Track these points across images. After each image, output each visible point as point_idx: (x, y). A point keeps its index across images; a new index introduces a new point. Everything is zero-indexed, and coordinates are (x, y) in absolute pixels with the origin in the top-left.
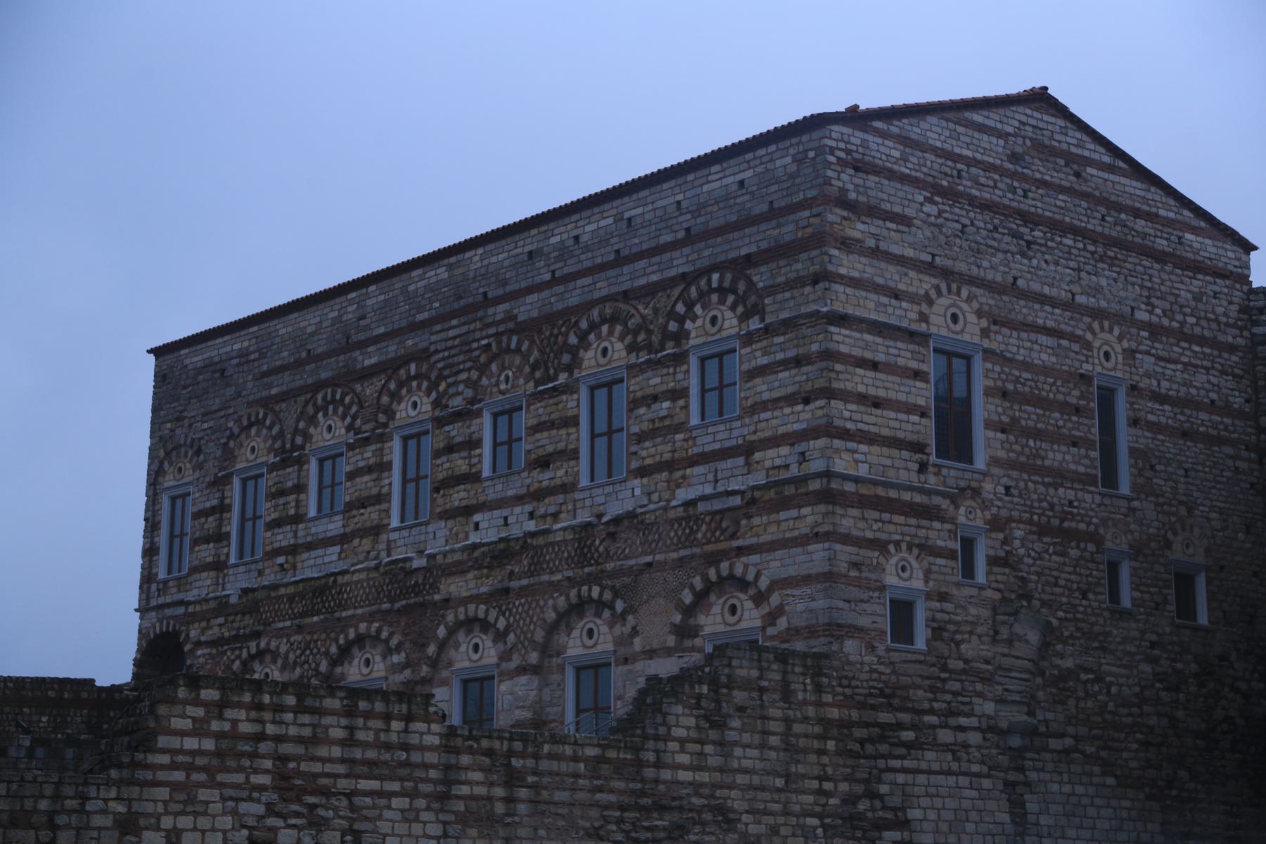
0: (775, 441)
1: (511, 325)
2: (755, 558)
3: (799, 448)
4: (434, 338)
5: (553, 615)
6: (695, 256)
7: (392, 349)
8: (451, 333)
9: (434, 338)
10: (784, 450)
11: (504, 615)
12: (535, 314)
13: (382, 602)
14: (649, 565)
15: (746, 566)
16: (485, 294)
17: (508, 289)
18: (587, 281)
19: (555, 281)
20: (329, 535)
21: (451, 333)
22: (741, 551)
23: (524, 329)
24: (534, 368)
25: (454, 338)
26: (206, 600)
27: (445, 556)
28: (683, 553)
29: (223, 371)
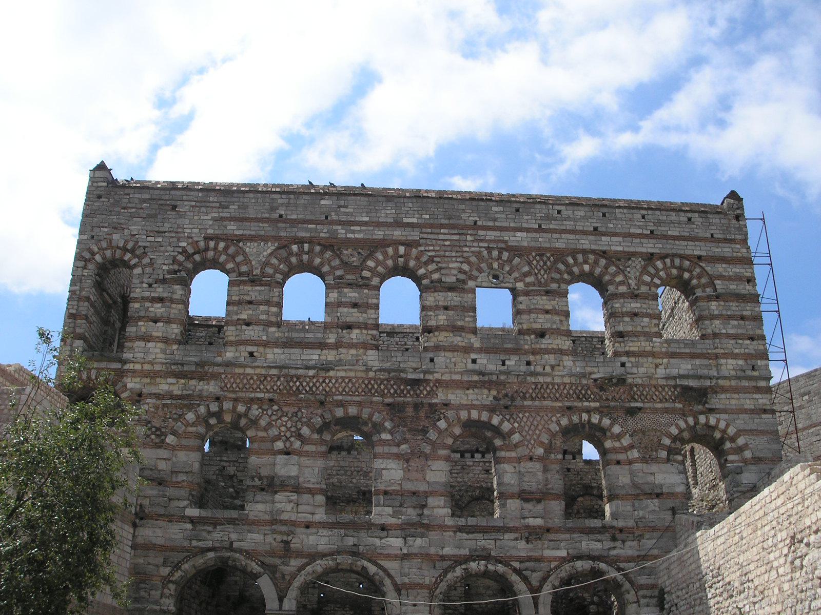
0: (736, 356)
1: (503, 245)
2: (726, 416)
3: (753, 362)
4: (425, 236)
5: (558, 429)
6: (661, 246)
7: (379, 234)
8: (441, 237)
9: (425, 236)
10: (741, 362)
11: (508, 421)
12: (525, 244)
13: (373, 395)
14: (640, 409)
15: (718, 420)
16: (475, 222)
17: (497, 224)
18: (572, 237)
19: (540, 229)
20: (306, 340)
21: (441, 237)
22: (711, 411)
23: (517, 251)
24: (526, 275)
25: (446, 240)
26: (151, 363)
27: (442, 374)
28: (667, 405)
29: (176, 206)
